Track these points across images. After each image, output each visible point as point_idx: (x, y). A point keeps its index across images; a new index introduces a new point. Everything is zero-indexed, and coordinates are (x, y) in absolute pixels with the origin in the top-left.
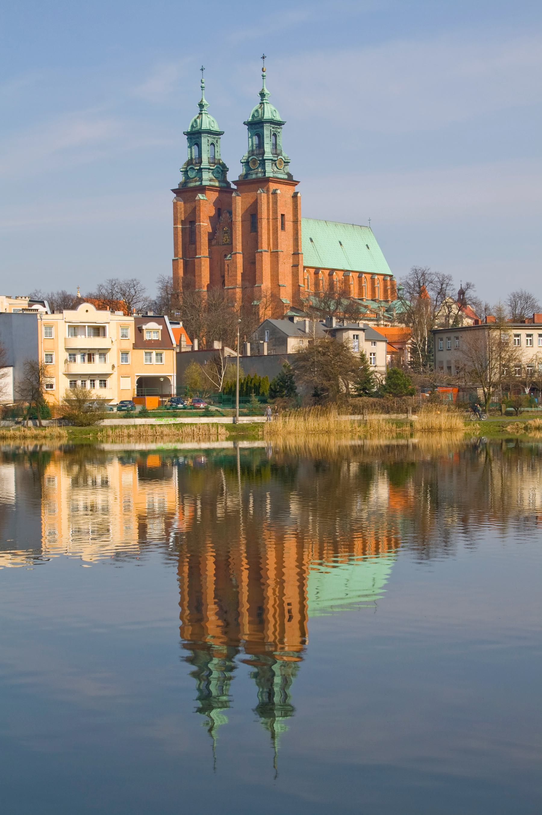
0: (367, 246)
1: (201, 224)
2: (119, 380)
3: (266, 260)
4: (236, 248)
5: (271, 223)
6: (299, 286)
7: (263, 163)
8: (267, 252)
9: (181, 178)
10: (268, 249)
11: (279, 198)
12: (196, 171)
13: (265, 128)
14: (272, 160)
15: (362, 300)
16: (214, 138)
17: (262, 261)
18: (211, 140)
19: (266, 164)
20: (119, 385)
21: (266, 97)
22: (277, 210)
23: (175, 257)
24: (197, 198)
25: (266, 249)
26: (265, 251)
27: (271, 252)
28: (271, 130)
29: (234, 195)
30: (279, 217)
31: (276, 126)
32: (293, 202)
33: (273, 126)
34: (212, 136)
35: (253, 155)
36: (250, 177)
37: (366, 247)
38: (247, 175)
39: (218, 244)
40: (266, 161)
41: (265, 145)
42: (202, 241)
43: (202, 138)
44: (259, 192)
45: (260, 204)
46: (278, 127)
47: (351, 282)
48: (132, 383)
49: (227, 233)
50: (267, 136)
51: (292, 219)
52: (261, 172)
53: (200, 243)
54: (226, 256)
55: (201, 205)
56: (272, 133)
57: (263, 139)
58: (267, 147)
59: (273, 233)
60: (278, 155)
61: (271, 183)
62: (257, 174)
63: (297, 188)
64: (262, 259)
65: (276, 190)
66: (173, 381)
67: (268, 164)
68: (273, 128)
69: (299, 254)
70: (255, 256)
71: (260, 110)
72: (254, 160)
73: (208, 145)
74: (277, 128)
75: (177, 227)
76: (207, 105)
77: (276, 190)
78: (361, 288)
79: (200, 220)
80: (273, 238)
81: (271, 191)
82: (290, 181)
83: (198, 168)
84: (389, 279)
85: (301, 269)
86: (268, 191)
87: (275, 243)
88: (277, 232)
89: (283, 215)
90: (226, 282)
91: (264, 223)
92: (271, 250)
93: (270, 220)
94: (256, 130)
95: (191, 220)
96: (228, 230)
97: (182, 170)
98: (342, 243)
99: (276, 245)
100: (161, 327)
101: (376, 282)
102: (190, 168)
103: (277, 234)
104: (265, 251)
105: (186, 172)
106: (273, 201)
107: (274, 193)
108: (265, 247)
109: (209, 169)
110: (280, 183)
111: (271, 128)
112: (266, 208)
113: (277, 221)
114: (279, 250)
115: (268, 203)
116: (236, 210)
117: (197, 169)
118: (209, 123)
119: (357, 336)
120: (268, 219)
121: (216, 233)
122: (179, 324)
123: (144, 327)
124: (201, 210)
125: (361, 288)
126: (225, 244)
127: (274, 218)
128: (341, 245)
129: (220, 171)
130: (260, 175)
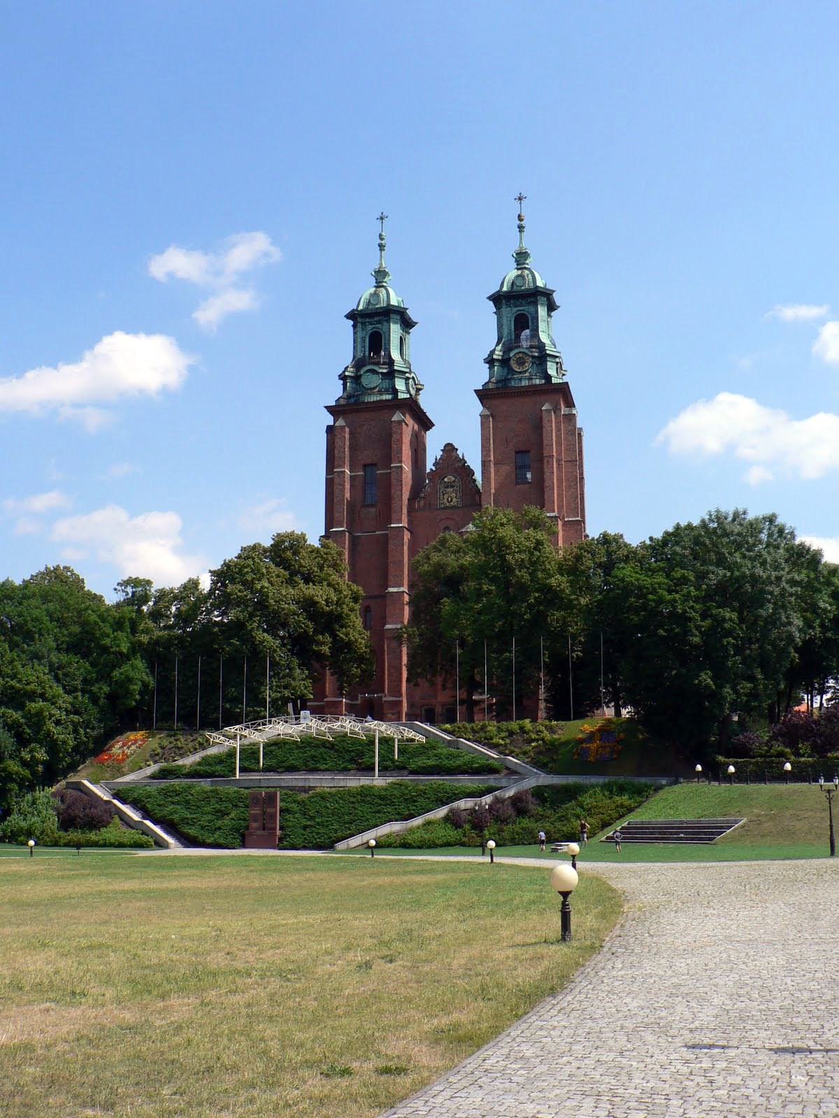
40: (548, 359)
49: (452, 487)
72: (521, 355)
83: (385, 371)
94: (517, 309)
96: (454, 481)
102: (368, 371)
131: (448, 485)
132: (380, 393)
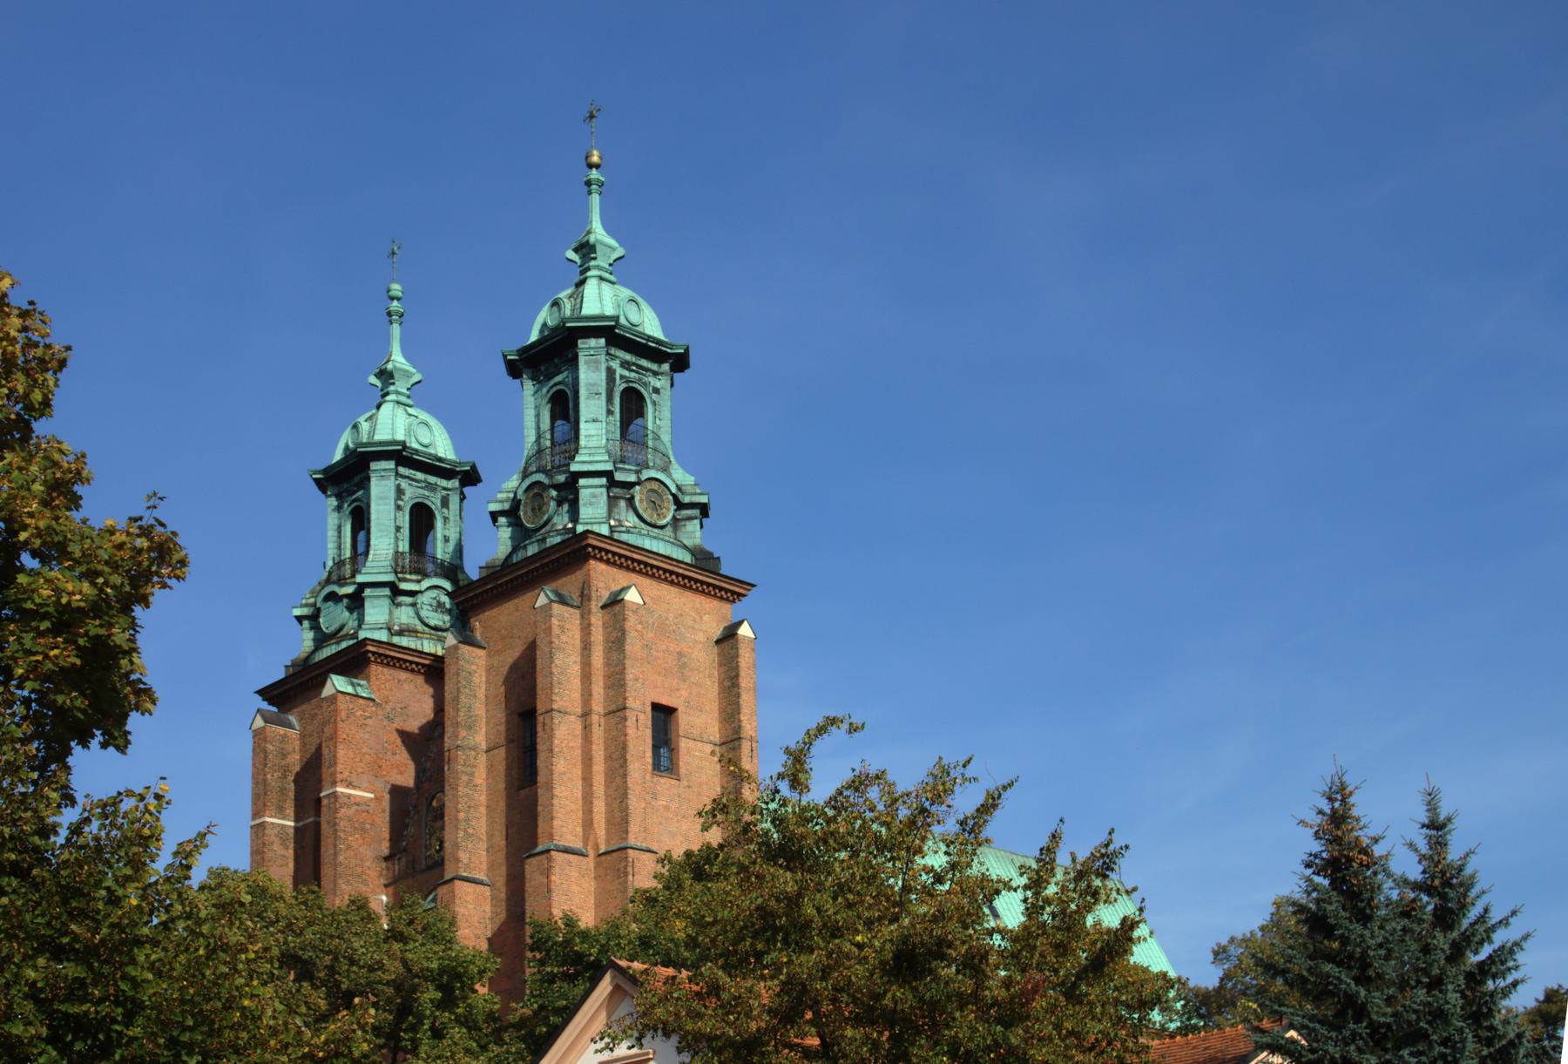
4: (458, 860)
5: (598, 734)
7: (569, 492)
8: (584, 855)
10: (586, 841)
11: (632, 622)
12: (345, 601)
13: (582, 360)
16: (431, 487)
17: (549, 891)
18: (412, 493)
19: (584, 494)
21: (599, 254)
22: (623, 672)
24: (327, 691)
25: (577, 844)
26: (566, 851)
27: (600, 855)
28: (610, 372)
31: (644, 363)
32: (721, 665)
33: (628, 357)
34: (420, 476)
40: (582, 482)
41: (582, 425)
42: (341, 858)
43: (374, 482)
44: (542, 600)
45: (546, 649)
46: (654, 367)
50: (594, 390)
51: (714, 732)
53: (335, 865)
55: (343, 715)
56: (620, 386)
58: (593, 432)
61: (592, 562)
64: (549, 882)
65: (625, 589)
68: (625, 365)
73: (399, 508)
74: (647, 370)
76: (408, 375)
79: (334, 774)
80: (607, 795)
83: (350, 590)
86: (585, 596)
87: (617, 814)
89: (663, 714)
92: (597, 847)
93: (595, 718)
97: (297, 612)
99: (620, 820)
103: (625, 776)
106: (607, 641)
107: (615, 602)
111: (615, 365)
112: (575, 669)
113: (625, 719)
115: (586, 646)
116: (456, 700)
117: (347, 596)
120: (586, 715)
121: (406, 826)
124: (342, 735)
127: (613, 707)
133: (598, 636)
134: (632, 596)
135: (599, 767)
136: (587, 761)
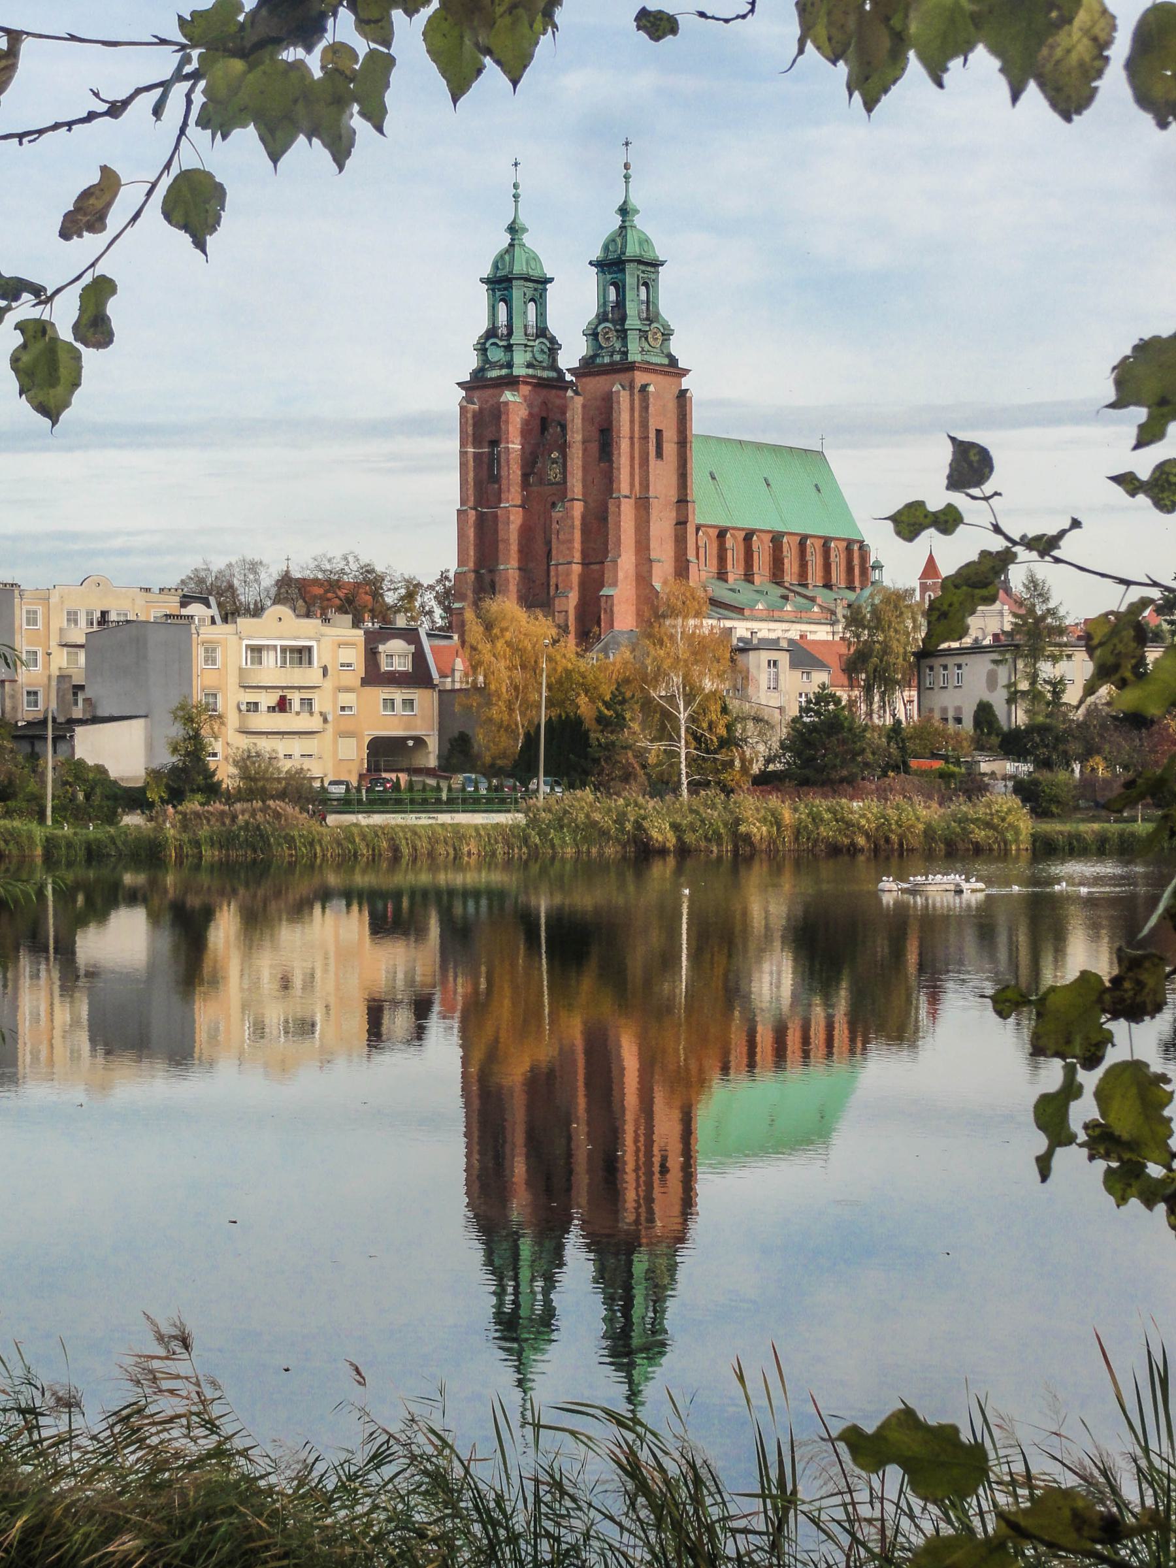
0: (816, 486)
1: (510, 446)
2: (335, 743)
3: (627, 513)
5: (637, 446)
6: (688, 561)
7: (623, 334)
9: (472, 361)
11: (651, 400)
14: (640, 330)
15: (805, 586)
19: (629, 337)
20: (335, 752)
23: (462, 505)
25: (628, 494)
26: (626, 497)
29: (570, 393)
30: (652, 435)
35: (606, 320)
36: (598, 360)
37: (814, 489)
38: (594, 357)
39: (541, 482)
47: (785, 553)
48: (359, 748)
51: (675, 439)
52: (620, 352)
54: (554, 505)
57: (624, 292)
59: (641, 467)
60: (652, 322)
61: (637, 373)
62: (612, 356)
63: (685, 383)
66: (433, 744)
67: (632, 337)
68: (643, 272)
69: (687, 502)
70: (607, 504)
71: (619, 240)
75: (466, 452)
77: (647, 385)
78: (803, 565)
79: (507, 438)
81: (638, 385)
82: (673, 369)
84: (856, 547)
85: (691, 529)
86: (632, 388)
88: (648, 461)
89: (659, 432)
90: (554, 552)
91: (625, 445)
93: (636, 440)
95: (494, 438)
98: (770, 482)
99: (645, 485)
100: (412, 648)
101: (833, 554)
104: (626, 497)
105: (482, 349)
106: (640, 405)
107: (644, 388)
108: (625, 488)
109: (526, 346)
110: (655, 371)
114: (651, 494)
115: (632, 409)
118: (527, 263)
119: (775, 662)
120: (632, 438)
122: (450, 638)
123: (381, 648)
125: (803, 565)
126: (553, 484)
128: (768, 485)
129: (546, 350)
130: (617, 357)
131: (554, 462)
132: (502, 367)
133: (637, 402)
134: (651, 389)
135: (637, 462)
136: (632, 458)
